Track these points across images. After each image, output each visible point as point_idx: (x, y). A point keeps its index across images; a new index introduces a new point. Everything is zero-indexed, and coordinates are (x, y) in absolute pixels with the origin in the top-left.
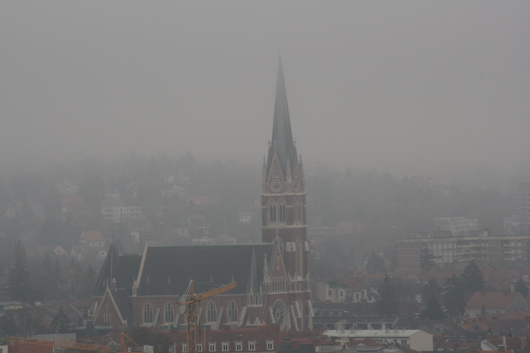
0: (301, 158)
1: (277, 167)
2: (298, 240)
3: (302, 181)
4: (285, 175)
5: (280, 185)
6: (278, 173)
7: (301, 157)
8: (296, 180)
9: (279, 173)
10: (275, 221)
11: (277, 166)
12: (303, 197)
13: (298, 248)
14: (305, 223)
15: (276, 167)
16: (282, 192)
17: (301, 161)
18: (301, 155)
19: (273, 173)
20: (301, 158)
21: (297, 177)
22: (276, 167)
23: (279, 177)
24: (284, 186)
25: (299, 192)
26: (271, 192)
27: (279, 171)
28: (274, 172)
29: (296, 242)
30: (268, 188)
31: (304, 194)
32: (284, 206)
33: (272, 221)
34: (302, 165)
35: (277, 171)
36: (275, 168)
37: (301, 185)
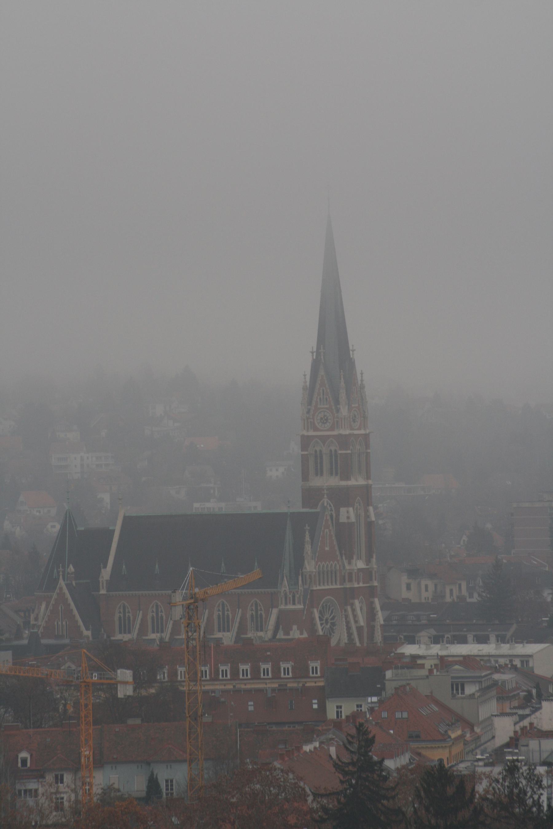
0: (362, 377)
1: (325, 391)
2: (358, 505)
6: (327, 399)
7: (362, 374)
9: (328, 399)
11: (324, 388)
12: (366, 437)
13: (358, 516)
17: (362, 380)
18: (362, 371)
19: (318, 400)
20: (362, 377)
23: (327, 406)
25: (359, 429)
27: (327, 397)
28: (320, 399)
29: (355, 507)
32: (336, 451)
36: (321, 391)
37: (362, 418)
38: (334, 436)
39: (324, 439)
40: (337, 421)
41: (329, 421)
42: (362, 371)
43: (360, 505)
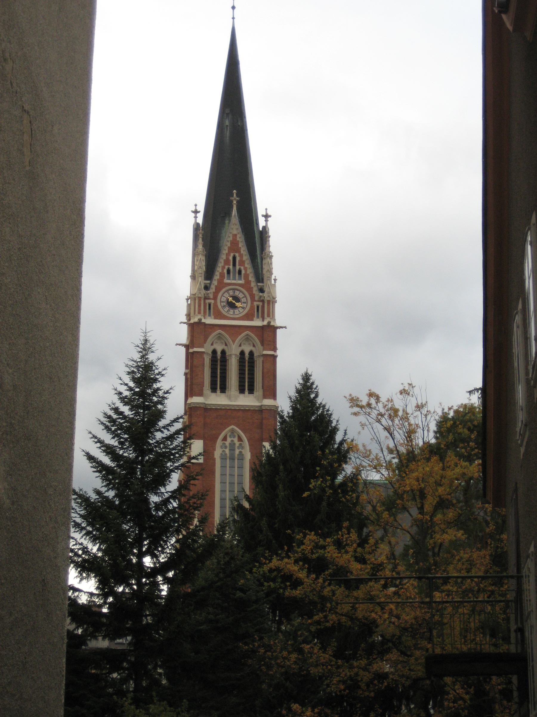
1: (238, 259)
6: (240, 272)
9: (243, 272)
11: (237, 255)
15: (234, 258)
22: (234, 258)
23: (242, 282)
24: (256, 303)
27: (242, 268)
35: (238, 267)
36: (231, 258)
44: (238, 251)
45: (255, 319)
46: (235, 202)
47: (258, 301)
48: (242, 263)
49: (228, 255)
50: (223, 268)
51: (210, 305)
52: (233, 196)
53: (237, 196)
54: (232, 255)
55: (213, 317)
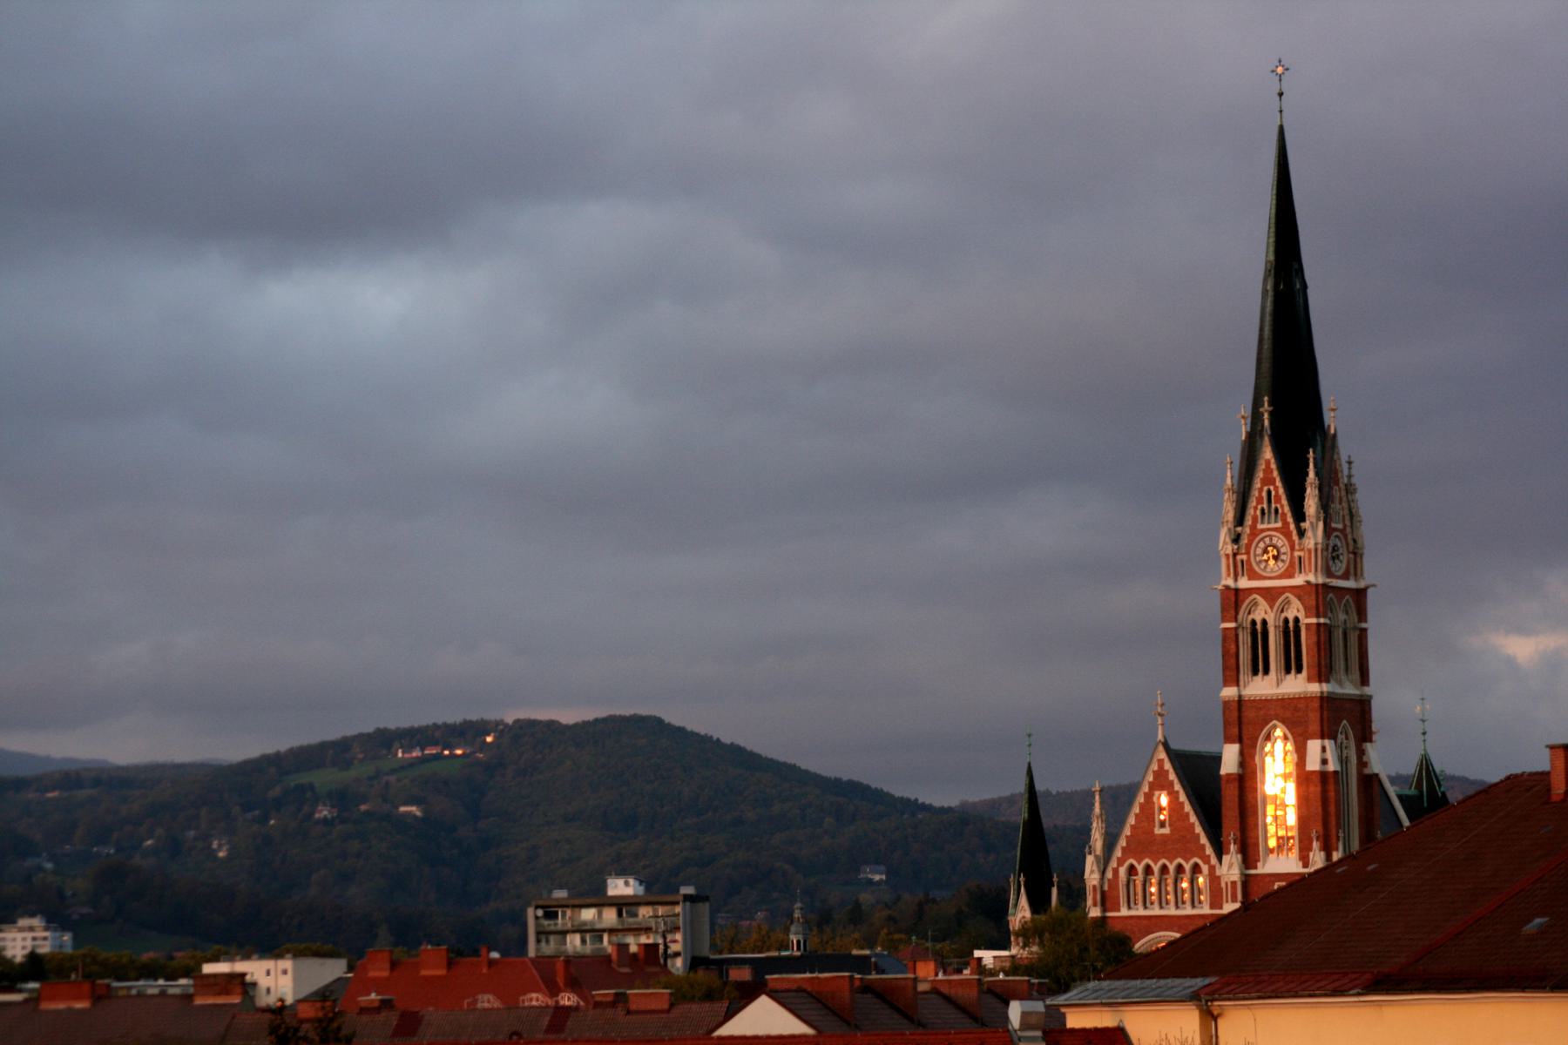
0: (1350, 468)
1: (1273, 493)
2: (1344, 737)
3: (1355, 541)
4: (1299, 516)
5: (1283, 550)
7: (1350, 463)
8: (1337, 536)
10: (1266, 671)
12: (1360, 595)
13: (1343, 761)
14: (1364, 679)
15: (1269, 492)
16: (1288, 574)
17: (1350, 476)
18: (1349, 457)
20: (1350, 468)
21: (1340, 526)
22: (1269, 492)
23: (1279, 525)
24: (1297, 554)
25: (1346, 576)
26: (1253, 575)
29: (1339, 741)
30: (1242, 561)
31: (1362, 584)
32: (1297, 620)
33: (1255, 672)
34: (1355, 490)
38: (1292, 589)
39: (1271, 595)
40: (1300, 558)
41: (1283, 557)
42: (1349, 457)
43: (1347, 738)
44: (1273, 482)
45: (1296, 575)
46: (1266, 416)
47: (1299, 550)
48: (1278, 499)
49: (1261, 490)
50: (1256, 508)
51: (1242, 561)
52: (1263, 405)
53: (1269, 405)
54: (1266, 488)
55: (1246, 578)
